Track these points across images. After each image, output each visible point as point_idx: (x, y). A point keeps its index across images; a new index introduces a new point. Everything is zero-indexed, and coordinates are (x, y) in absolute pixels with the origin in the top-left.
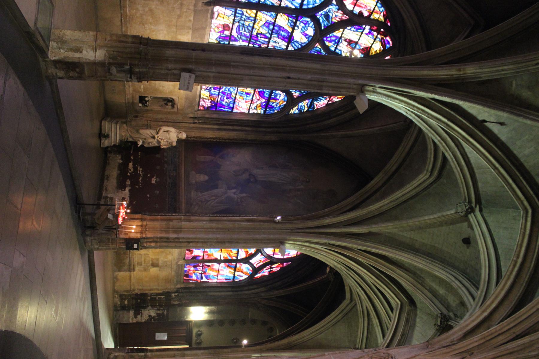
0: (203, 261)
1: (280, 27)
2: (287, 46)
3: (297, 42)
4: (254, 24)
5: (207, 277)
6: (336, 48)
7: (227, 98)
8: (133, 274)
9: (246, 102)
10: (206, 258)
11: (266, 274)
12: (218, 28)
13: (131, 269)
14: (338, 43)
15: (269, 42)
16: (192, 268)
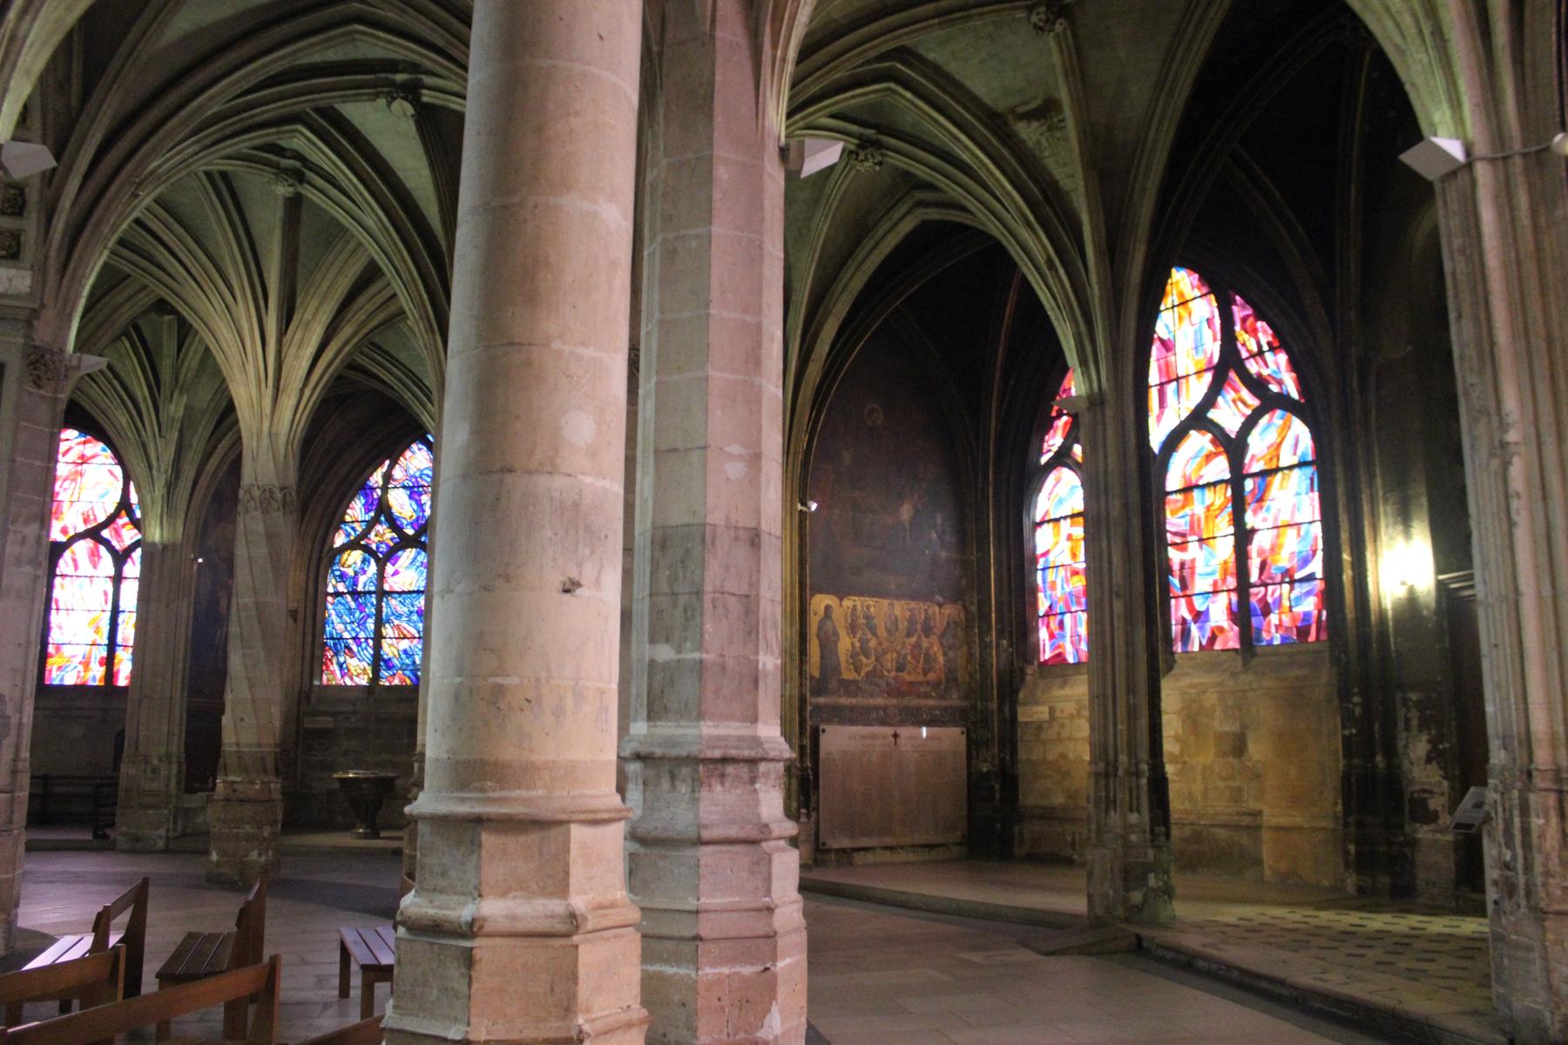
0: (1243, 587)
5: (1305, 561)
8: (1271, 817)
10: (1232, 582)
11: (1282, 358)
13: (1252, 826)
16: (1274, 618)
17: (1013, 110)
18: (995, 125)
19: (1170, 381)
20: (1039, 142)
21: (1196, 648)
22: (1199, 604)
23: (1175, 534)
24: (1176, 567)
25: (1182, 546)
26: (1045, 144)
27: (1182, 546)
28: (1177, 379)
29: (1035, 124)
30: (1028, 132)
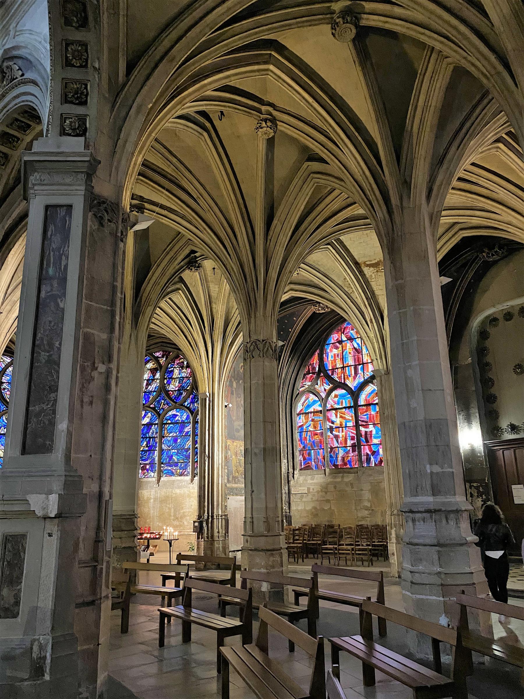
2: (155, 424)
12: (144, 473)
17: (365, 263)
18: (357, 266)
19: (360, 365)
20: (371, 276)
21: (373, 465)
22: (374, 448)
23: (363, 421)
24: (363, 434)
25: (366, 426)
26: (374, 277)
27: (366, 426)
28: (363, 364)
29: (372, 269)
30: (368, 271)
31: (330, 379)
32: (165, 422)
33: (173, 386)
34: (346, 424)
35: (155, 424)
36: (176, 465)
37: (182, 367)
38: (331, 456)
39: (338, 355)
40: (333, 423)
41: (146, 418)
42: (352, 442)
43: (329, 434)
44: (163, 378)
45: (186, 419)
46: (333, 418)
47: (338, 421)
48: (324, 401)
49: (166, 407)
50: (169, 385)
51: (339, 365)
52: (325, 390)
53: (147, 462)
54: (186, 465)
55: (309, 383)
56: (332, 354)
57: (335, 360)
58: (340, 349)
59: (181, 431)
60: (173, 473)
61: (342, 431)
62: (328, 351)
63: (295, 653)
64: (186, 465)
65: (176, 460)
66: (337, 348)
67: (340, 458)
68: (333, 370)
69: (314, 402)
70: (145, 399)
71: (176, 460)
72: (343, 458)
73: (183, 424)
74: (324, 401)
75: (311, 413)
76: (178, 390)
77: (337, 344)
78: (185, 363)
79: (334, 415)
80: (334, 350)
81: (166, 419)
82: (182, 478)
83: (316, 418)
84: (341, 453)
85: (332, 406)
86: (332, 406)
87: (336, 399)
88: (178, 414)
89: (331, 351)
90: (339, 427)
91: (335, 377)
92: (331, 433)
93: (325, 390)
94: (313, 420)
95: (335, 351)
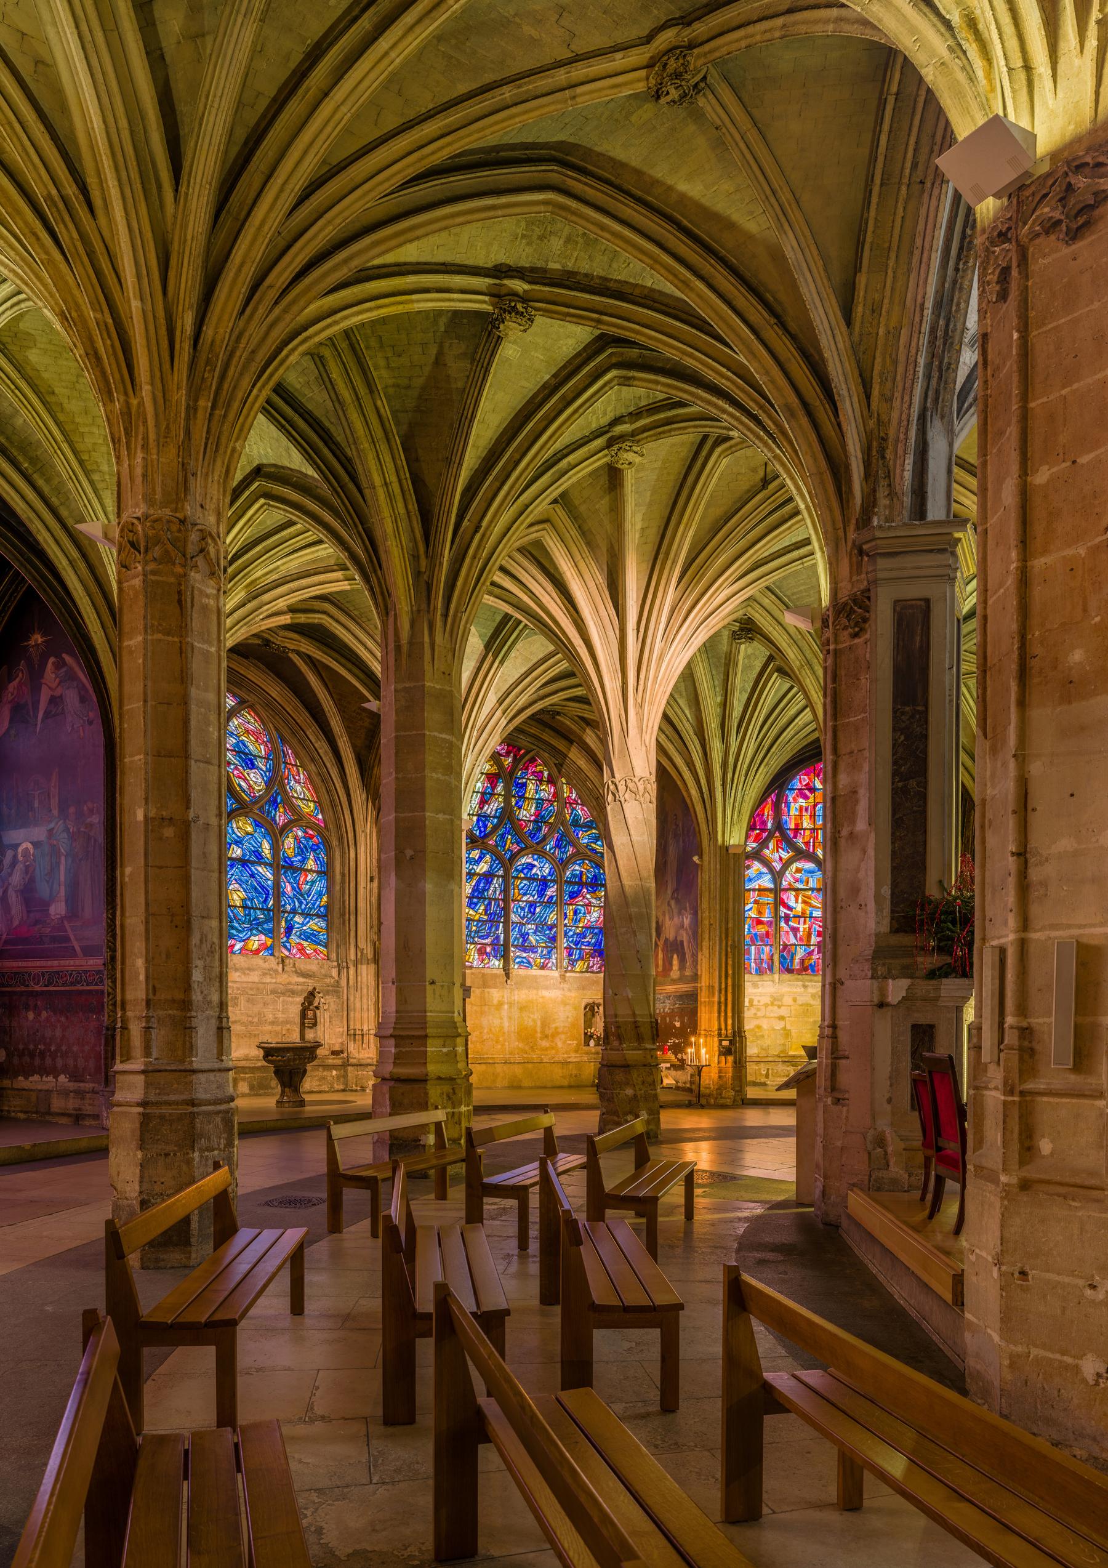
1: (474, 891)
2: (498, 876)
3: (491, 867)
4: (473, 920)
6: (494, 817)
7: (585, 937)
9: (589, 913)
12: (483, 960)
14: (487, 817)
15: (495, 899)
31: (791, 845)
32: (515, 874)
33: (526, 813)
34: (811, 913)
35: (498, 876)
36: (533, 949)
37: (541, 781)
38: (782, 957)
39: (806, 810)
40: (790, 908)
41: (482, 864)
42: (819, 939)
43: (783, 924)
44: (507, 797)
45: (549, 874)
46: (792, 902)
47: (799, 907)
48: (777, 876)
49: (515, 848)
50: (520, 808)
51: (806, 823)
52: (781, 859)
53: (486, 941)
54: (549, 952)
55: (754, 845)
56: (797, 806)
57: (801, 816)
58: (811, 800)
59: (541, 893)
60: (529, 963)
61: (805, 923)
62: (791, 799)
63: (308, 1322)
64: (549, 952)
65: (534, 942)
66: (806, 798)
67: (797, 961)
68: (797, 830)
69: (760, 874)
70: (479, 828)
71: (534, 942)
72: (802, 961)
73: (544, 883)
74: (777, 876)
75: (754, 890)
76: (534, 821)
77: (807, 792)
78: (546, 774)
79: (793, 898)
80: (801, 800)
81: (517, 870)
82: (543, 972)
83: (764, 900)
84: (800, 953)
85: (790, 884)
86: (790, 884)
87: (798, 875)
88: (535, 863)
89: (795, 800)
90: (799, 917)
91: (800, 842)
92: (787, 922)
93: (781, 859)
94: (756, 902)
95: (802, 802)
